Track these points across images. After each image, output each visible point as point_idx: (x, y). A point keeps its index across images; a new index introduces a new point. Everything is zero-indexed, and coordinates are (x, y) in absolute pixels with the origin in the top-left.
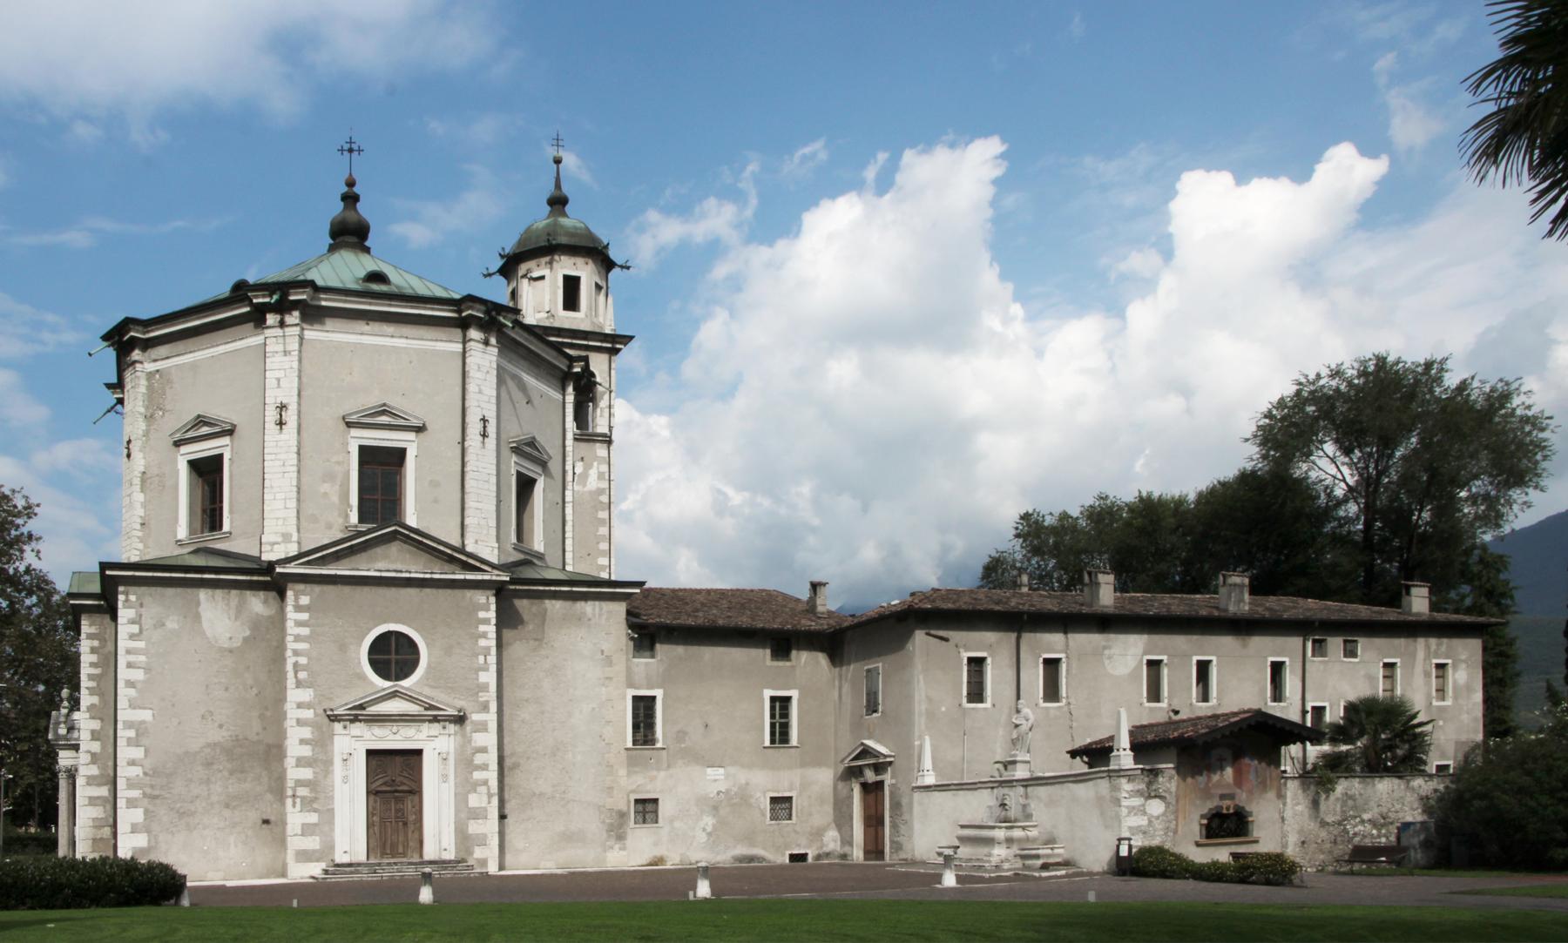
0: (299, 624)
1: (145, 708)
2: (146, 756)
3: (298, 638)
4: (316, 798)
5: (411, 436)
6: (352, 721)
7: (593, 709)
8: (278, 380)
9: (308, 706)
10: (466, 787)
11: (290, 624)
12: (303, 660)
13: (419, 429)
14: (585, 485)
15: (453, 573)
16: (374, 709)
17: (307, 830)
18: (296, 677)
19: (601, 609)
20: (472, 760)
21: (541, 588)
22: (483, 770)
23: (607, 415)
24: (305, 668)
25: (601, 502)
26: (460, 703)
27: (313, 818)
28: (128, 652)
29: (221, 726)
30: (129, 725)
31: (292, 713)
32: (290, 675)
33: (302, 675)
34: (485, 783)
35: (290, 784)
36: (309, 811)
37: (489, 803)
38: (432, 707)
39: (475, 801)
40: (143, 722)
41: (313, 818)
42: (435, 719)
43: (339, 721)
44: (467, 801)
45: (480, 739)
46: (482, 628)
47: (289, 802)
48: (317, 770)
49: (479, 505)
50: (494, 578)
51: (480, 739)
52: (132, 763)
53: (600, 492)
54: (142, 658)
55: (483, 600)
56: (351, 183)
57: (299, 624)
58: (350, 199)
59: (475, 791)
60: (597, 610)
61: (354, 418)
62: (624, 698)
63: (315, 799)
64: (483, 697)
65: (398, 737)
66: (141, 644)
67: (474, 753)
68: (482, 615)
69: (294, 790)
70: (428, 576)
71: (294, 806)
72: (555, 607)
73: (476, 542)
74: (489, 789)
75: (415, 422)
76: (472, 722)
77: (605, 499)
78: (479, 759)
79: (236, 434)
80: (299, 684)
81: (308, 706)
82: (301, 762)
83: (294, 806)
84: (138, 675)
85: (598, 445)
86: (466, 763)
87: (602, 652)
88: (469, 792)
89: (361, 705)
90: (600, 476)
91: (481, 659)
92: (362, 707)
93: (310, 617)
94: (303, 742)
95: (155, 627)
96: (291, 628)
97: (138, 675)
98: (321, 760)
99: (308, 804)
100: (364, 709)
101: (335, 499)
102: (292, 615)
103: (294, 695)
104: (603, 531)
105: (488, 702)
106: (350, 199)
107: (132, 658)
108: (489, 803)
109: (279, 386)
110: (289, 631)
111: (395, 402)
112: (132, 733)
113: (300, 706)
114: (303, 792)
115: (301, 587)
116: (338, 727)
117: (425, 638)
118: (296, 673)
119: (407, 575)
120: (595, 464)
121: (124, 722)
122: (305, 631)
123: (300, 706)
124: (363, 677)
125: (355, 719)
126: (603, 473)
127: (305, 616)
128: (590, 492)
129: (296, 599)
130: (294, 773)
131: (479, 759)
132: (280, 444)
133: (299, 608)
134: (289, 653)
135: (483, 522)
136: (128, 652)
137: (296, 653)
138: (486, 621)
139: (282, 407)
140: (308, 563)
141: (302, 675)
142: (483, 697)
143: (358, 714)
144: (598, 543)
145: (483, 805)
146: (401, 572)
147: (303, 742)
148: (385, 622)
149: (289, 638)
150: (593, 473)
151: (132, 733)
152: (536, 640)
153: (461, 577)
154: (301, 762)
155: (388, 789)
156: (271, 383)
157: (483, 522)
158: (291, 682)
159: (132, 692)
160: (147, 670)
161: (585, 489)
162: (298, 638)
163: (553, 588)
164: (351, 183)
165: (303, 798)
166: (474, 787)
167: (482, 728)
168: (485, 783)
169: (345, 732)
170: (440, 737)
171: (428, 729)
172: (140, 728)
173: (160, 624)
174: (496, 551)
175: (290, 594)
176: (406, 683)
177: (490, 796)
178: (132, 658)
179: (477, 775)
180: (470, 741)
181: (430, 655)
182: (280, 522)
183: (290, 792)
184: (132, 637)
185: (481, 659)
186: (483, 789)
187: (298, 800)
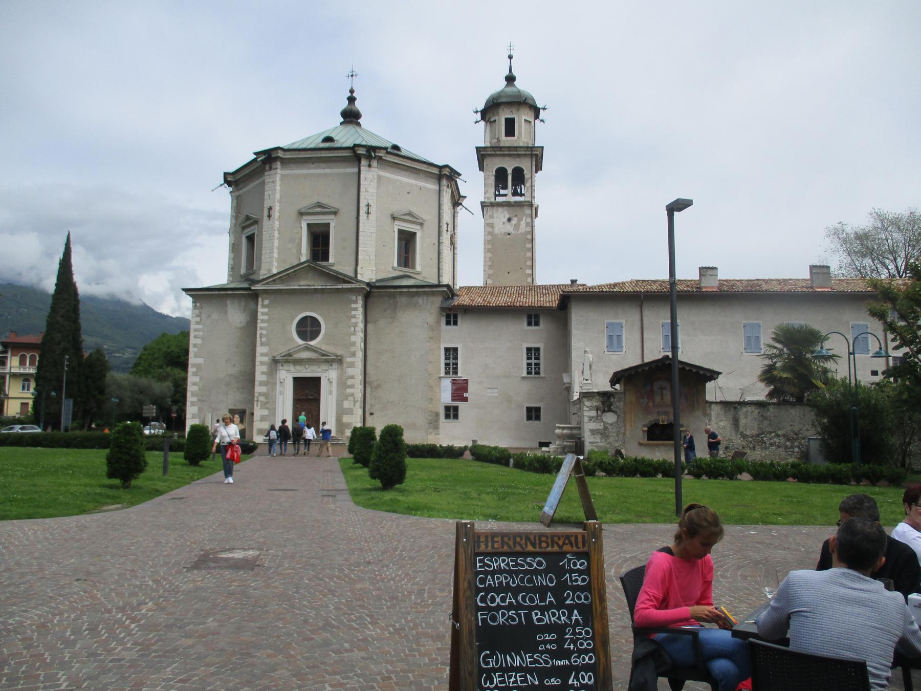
0: (263, 314)
1: (201, 357)
2: (200, 381)
3: (263, 321)
4: (268, 402)
5: (332, 217)
6: (285, 362)
7: (422, 355)
8: (269, 195)
9: (266, 355)
10: (342, 397)
11: (259, 314)
12: (264, 332)
13: (335, 213)
14: (518, 230)
15: (336, 285)
16: (297, 356)
17: (263, 418)
18: (261, 340)
19: (427, 300)
20: (346, 383)
21: (392, 290)
22: (351, 388)
23: (530, 190)
24: (265, 336)
25: (527, 239)
26: (339, 352)
27: (266, 412)
28: (195, 330)
29: (234, 366)
30: (194, 365)
31: (259, 359)
32: (258, 339)
33: (264, 339)
34: (352, 395)
35: (256, 395)
36: (264, 409)
37: (354, 406)
38: (323, 355)
39: (347, 404)
40: (199, 364)
41: (266, 412)
42: (327, 361)
43: (279, 362)
44: (342, 405)
45: (350, 371)
46: (353, 313)
47: (255, 403)
48: (269, 388)
49: (365, 249)
50: (358, 286)
51: (350, 371)
52: (194, 384)
53: (527, 233)
54: (201, 333)
55: (354, 298)
56: (352, 91)
57: (263, 314)
58: (352, 100)
59: (347, 399)
60: (425, 301)
61: (303, 210)
62: (440, 349)
63: (267, 403)
64: (353, 349)
65: (308, 370)
66: (200, 327)
67: (347, 379)
68: (353, 306)
69: (258, 398)
70: (324, 287)
71: (257, 406)
72: (402, 300)
73: (362, 268)
74: (354, 399)
75: (333, 210)
76: (347, 362)
77: (529, 237)
78: (350, 382)
79: (259, 223)
80: (262, 344)
81: (266, 355)
82: (262, 384)
83: (257, 406)
84: (199, 341)
85: (526, 207)
86: (343, 384)
87: (428, 324)
88: (344, 400)
89: (289, 354)
90: (527, 224)
91: (352, 329)
92: (290, 355)
93: (269, 310)
94: (263, 373)
95: (207, 318)
96: (260, 317)
97: (199, 341)
98: (271, 383)
99: (264, 405)
100: (291, 356)
101: (294, 251)
102: (260, 310)
103: (260, 349)
104: (529, 254)
105: (355, 351)
106: (352, 100)
107: (196, 333)
108: (354, 406)
109: (269, 198)
110: (259, 318)
111: (325, 201)
112: (194, 370)
113: (262, 355)
114: (262, 399)
115: (265, 296)
116: (279, 366)
117: (324, 319)
118: (261, 338)
119: (314, 287)
120: (524, 218)
121: (192, 364)
122: (266, 317)
123: (262, 355)
124: (292, 340)
125: (287, 361)
126: (529, 223)
127: (266, 310)
128: (521, 233)
129: (263, 302)
130: (258, 389)
131: (350, 382)
132: (269, 226)
133: (263, 306)
134: (258, 329)
135: (367, 258)
136: (195, 330)
137: (261, 328)
138: (356, 309)
139: (270, 209)
140: (267, 283)
141: (264, 339)
142: (353, 349)
143: (288, 359)
144: (526, 262)
145: (352, 407)
146: (310, 286)
147: (263, 373)
148: (304, 311)
149: (259, 321)
150: (523, 223)
151: (194, 370)
152: (391, 318)
153: (341, 287)
154: (262, 384)
155: (305, 398)
156: (266, 197)
157: (367, 258)
158: (258, 343)
159: (196, 349)
160: (203, 339)
161: (519, 232)
162: (263, 321)
163: (398, 290)
164: (352, 91)
165: (262, 402)
166: (346, 397)
167: (352, 365)
168: (352, 395)
169: (281, 368)
170: (330, 371)
171: (324, 367)
172: (198, 366)
173: (210, 317)
174: (374, 272)
175: (260, 299)
176: (312, 343)
177: (355, 402)
178: (196, 333)
179: (349, 391)
180: (345, 373)
181: (326, 328)
182: (268, 264)
183: (256, 399)
184: (197, 323)
185: (352, 329)
186: (351, 398)
187: (259, 403)
